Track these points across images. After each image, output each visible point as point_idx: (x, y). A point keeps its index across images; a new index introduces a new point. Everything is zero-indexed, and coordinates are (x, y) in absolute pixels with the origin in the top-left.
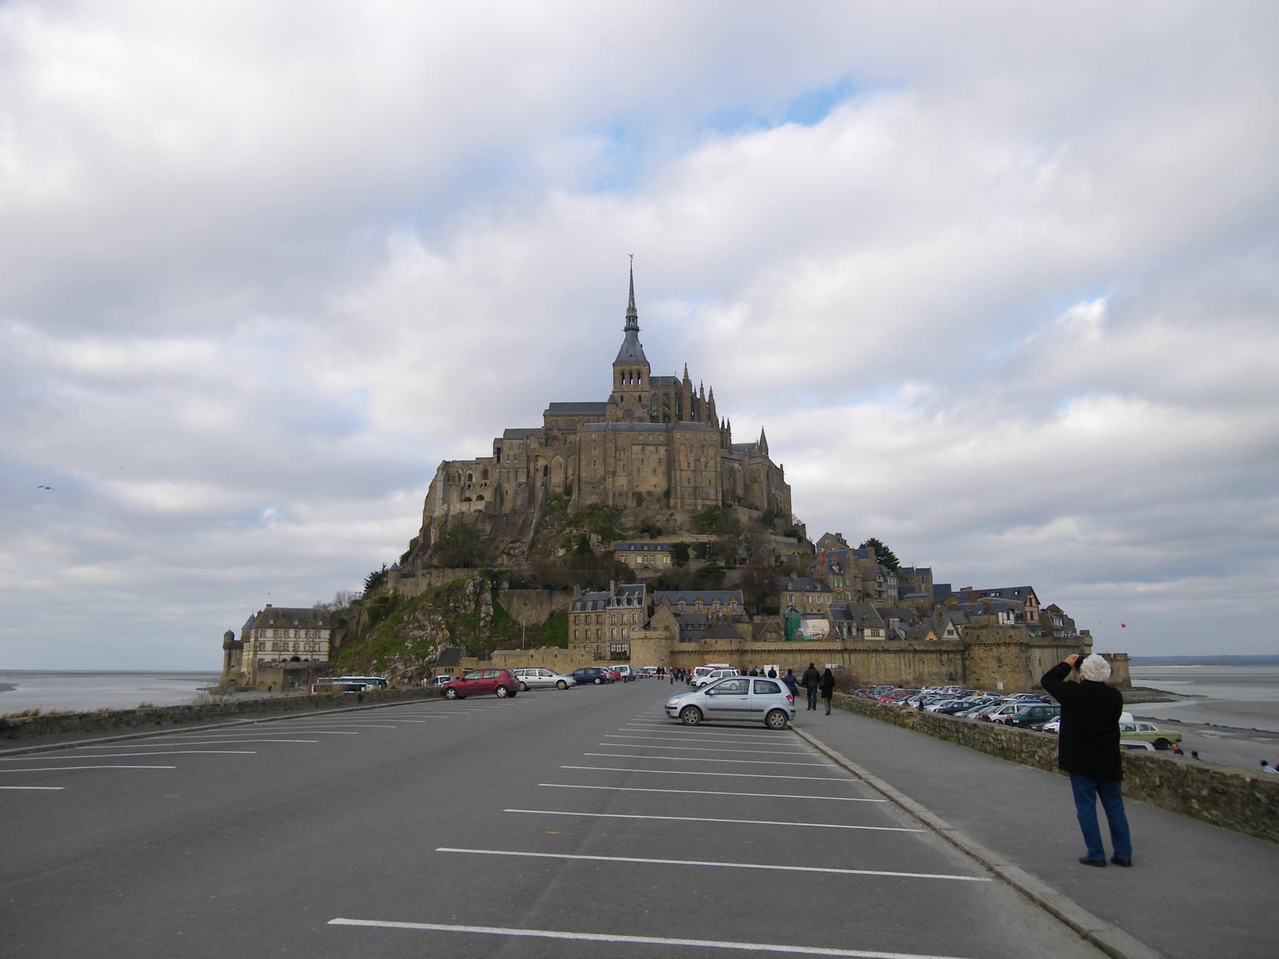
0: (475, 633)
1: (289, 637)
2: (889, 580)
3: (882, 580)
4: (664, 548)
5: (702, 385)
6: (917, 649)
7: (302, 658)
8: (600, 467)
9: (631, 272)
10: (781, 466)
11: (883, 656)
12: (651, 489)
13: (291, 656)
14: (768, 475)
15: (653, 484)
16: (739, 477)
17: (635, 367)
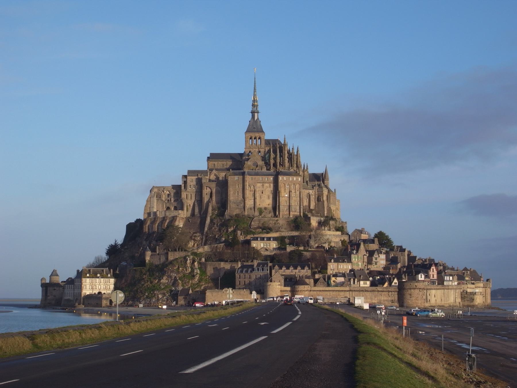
0: (192, 282)
1: (96, 282)
2: (381, 256)
3: (377, 256)
4: (275, 239)
5: (293, 147)
6: (379, 290)
7: (103, 292)
8: (241, 194)
9: (255, 79)
10: (335, 189)
11: (365, 293)
12: (266, 206)
13: (98, 292)
14: (327, 196)
15: (268, 203)
16: (313, 198)
17: (257, 135)
